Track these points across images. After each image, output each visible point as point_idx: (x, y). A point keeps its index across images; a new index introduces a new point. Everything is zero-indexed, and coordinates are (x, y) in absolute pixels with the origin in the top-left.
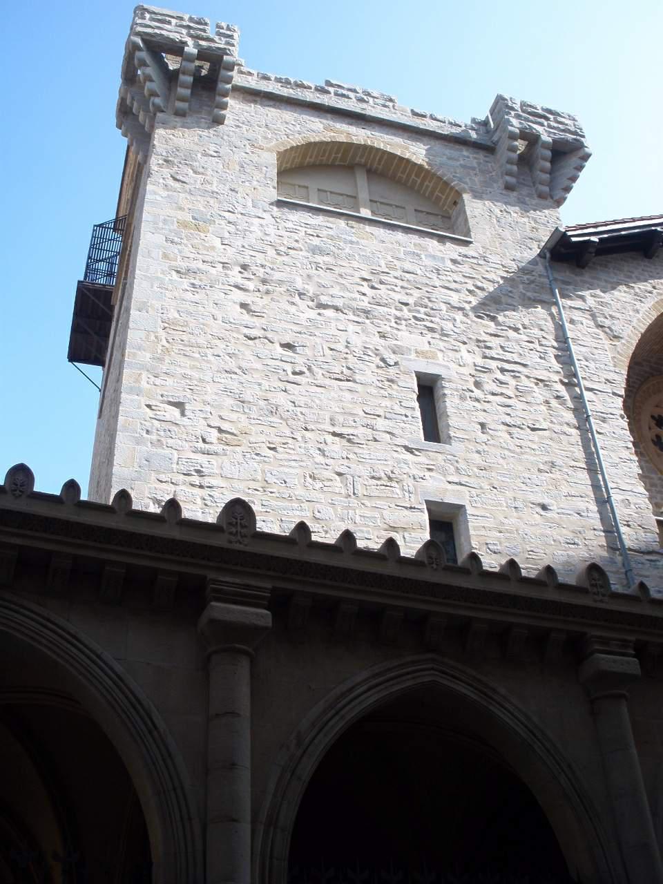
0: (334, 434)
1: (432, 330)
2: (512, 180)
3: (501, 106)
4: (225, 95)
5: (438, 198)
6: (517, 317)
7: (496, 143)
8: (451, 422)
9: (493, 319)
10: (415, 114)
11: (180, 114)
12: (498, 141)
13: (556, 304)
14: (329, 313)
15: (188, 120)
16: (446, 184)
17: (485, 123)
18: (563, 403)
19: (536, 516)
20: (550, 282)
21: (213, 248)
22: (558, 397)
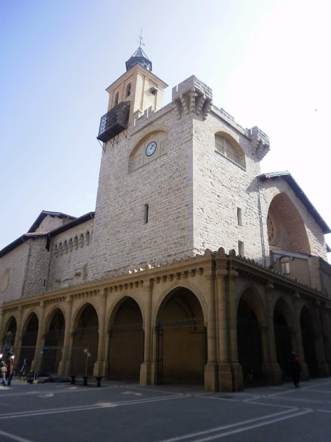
0: (226, 221)
1: (239, 195)
2: (254, 152)
3: (255, 129)
4: (208, 113)
5: (238, 152)
6: (252, 194)
7: (252, 140)
8: (267, 236)
9: (249, 194)
10: (238, 125)
11: (197, 115)
12: (252, 140)
13: (259, 192)
14: (224, 187)
15: (199, 117)
16: (242, 150)
17: (249, 131)
18: (258, 219)
19: (252, 246)
20: (258, 185)
22: (257, 217)
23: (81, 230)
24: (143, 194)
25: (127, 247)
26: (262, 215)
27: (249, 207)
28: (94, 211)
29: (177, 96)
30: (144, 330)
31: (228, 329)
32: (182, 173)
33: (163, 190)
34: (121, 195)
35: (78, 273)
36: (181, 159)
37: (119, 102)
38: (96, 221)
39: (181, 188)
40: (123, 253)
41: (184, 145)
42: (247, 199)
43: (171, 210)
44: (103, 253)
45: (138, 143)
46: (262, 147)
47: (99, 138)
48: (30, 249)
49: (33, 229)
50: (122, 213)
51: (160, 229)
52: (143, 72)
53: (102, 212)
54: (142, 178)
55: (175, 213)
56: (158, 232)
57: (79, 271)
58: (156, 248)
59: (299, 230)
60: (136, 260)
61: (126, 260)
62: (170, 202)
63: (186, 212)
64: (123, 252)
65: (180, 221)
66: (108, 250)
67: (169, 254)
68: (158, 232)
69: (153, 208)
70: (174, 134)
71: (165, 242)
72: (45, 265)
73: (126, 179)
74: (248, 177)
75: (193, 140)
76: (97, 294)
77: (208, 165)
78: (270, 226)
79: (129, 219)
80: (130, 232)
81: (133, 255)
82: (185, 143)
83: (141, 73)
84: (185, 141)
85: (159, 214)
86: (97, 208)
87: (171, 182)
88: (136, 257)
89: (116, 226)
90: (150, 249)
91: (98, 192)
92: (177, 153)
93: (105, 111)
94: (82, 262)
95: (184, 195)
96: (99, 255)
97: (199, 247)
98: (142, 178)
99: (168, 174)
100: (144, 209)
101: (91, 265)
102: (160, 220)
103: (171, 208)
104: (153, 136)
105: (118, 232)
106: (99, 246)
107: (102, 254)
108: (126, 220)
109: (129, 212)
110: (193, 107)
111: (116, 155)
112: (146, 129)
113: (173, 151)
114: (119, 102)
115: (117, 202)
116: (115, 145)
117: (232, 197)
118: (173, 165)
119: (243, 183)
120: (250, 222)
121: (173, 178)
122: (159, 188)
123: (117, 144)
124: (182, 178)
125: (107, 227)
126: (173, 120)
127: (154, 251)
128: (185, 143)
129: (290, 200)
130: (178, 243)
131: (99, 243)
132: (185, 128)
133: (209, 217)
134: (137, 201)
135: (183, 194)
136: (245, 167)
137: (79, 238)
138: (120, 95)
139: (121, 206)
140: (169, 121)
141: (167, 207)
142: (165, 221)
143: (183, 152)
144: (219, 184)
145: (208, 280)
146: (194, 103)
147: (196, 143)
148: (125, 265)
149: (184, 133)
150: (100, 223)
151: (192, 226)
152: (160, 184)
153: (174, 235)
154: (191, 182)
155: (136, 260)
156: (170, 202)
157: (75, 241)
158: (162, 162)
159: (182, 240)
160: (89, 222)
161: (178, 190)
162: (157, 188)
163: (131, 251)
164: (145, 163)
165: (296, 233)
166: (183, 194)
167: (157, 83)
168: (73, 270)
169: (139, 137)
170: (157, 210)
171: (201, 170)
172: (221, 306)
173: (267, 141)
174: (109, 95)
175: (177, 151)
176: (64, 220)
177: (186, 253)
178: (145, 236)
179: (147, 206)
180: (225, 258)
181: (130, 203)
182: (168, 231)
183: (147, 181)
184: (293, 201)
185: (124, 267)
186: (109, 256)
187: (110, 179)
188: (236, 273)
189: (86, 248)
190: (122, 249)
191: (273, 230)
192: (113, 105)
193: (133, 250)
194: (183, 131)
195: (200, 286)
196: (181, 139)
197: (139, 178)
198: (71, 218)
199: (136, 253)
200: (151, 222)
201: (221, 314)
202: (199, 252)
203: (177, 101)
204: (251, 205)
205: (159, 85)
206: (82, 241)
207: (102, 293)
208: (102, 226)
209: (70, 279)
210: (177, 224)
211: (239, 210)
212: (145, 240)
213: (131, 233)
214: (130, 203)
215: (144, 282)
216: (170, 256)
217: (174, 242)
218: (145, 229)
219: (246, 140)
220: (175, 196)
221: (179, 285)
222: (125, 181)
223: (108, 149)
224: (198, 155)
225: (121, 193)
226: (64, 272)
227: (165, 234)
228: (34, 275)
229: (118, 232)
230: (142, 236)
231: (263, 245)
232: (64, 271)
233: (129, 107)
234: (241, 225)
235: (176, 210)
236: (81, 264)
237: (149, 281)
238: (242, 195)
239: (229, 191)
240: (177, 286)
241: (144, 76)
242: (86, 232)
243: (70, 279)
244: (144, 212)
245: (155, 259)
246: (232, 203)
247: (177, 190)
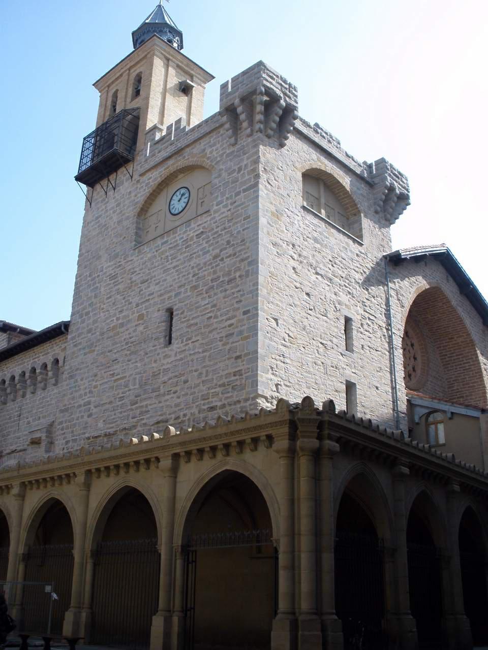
0: (321, 343)
1: (349, 293)
2: (379, 209)
3: (381, 163)
4: (288, 133)
5: (347, 208)
6: (374, 290)
7: (375, 184)
9: (367, 290)
10: (347, 155)
11: (269, 137)
12: (377, 184)
13: (387, 285)
14: (319, 277)
15: (271, 141)
16: (356, 205)
17: (370, 166)
18: (385, 339)
21: (282, 231)
22: (384, 335)
23: (43, 355)
24: (163, 287)
25: (130, 390)
26: (393, 330)
27: (367, 315)
28: (69, 320)
29: (230, 100)
30: (159, 551)
31: (317, 551)
32: (239, 249)
33: (200, 282)
34: (121, 290)
35: (36, 438)
36: (236, 223)
38: (73, 338)
39: (235, 278)
40: (123, 401)
41: (242, 195)
42: (365, 300)
43: (215, 320)
44: (86, 400)
45: (154, 188)
46: (395, 199)
47: (79, 178)
50: (122, 325)
51: (195, 357)
52: (165, 50)
53: (83, 322)
54: (162, 258)
55: (223, 326)
56: (190, 363)
57: (37, 435)
58: (187, 394)
59: (466, 360)
60: (148, 416)
61: (128, 415)
62: (215, 306)
63: (245, 325)
64: (123, 400)
65: (233, 343)
66: (94, 397)
67: (211, 405)
68: (190, 363)
69: (182, 316)
70: (224, 174)
71: (203, 382)
73: (130, 259)
74: (366, 257)
75: (260, 186)
76: (72, 482)
77: (289, 235)
78: (409, 351)
79: (136, 336)
80: (136, 362)
81: (142, 407)
82: (244, 191)
83: (162, 53)
84: (245, 187)
85: (193, 328)
86: (72, 315)
87: (217, 266)
88: (149, 411)
89: (110, 349)
90: (175, 395)
91: (76, 283)
92: (229, 210)
93: (91, 126)
94: (44, 417)
95: (241, 293)
96: (76, 405)
97: (268, 394)
98: (162, 258)
99: (211, 252)
100: (164, 318)
101: (61, 423)
102: (194, 339)
103: (216, 317)
104: (182, 175)
105: (113, 361)
106: (77, 388)
107: (82, 402)
108: (130, 338)
109: (137, 323)
110: (260, 122)
111: (111, 212)
112: (170, 162)
113: (221, 206)
115: (114, 304)
116: (111, 193)
117: (334, 296)
118: (220, 234)
119: (357, 269)
120: (370, 344)
121: (220, 258)
122: (194, 279)
123: (114, 189)
124: (238, 259)
125: (94, 351)
126: (221, 146)
127: (181, 399)
128: (243, 192)
129: (449, 302)
130: (228, 385)
131: (76, 381)
132: (245, 162)
133: (289, 336)
134: (152, 302)
135: (239, 291)
136: (361, 237)
137: (38, 371)
138: (121, 95)
139: (121, 312)
140: (214, 148)
141: (210, 315)
142: (204, 342)
143: (239, 208)
144: (309, 270)
145: (282, 459)
146: (262, 114)
147: (266, 192)
148: (127, 426)
149: (242, 172)
150: (80, 343)
151: (256, 352)
152: (196, 269)
153: (221, 368)
154: (255, 266)
155: (148, 416)
156: (215, 306)
157: (30, 377)
159: (237, 380)
160: (57, 340)
161: (230, 281)
162: (191, 279)
163: (139, 398)
164: (168, 229)
165: (461, 364)
166: (239, 291)
167: (192, 72)
168: (27, 432)
169: (156, 176)
170: (188, 320)
172: (305, 509)
173: (404, 188)
174: (100, 94)
175: (230, 207)
176: (9, 334)
177: (242, 404)
178: (166, 371)
179: (170, 312)
180: (315, 417)
181: (137, 305)
183: (172, 263)
184: (454, 303)
185: (125, 429)
186: (95, 407)
187: (99, 258)
188: (336, 446)
189: (53, 391)
190: (123, 393)
191: (415, 359)
192: (108, 113)
193: (143, 397)
194: (240, 169)
195: (265, 469)
196: (237, 183)
197: (155, 256)
198: (24, 332)
199: (148, 402)
200: (178, 343)
201: (305, 524)
202: (268, 402)
203: (229, 110)
204: (372, 312)
205: (196, 77)
206: (44, 377)
207: (81, 478)
208: (84, 348)
210: (228, 347)
211: (348, 320)
212: (166, 378)
213: (139, 365)
214: (137, 305)
215: (161, 460)
216: (212, 409)
217: (221, 382)
218: (166, 355)
219: (363, 186)
220: (223, 294)
221: (228, 467)
222: (127, 262)
223: (96, 199)
224: (270, 215)
225: (121, 287)
226: (9, 437)
227: (205, 367)
229: (113, 361)
230: (160, 370)
231: (394, 388)
232: (9, 435)
233: (137, 118)
234: (352, 351)
235: (226, 321)
237: (170, 458)
238: (355, 293)
239: (329, 284)
240: (224, 469)
241: (168, 60)
242: (52, 360)
243: (21, 451)
244: (163, 324)
245: (185, 415)
246: (335, 307)
247: (228, 282)
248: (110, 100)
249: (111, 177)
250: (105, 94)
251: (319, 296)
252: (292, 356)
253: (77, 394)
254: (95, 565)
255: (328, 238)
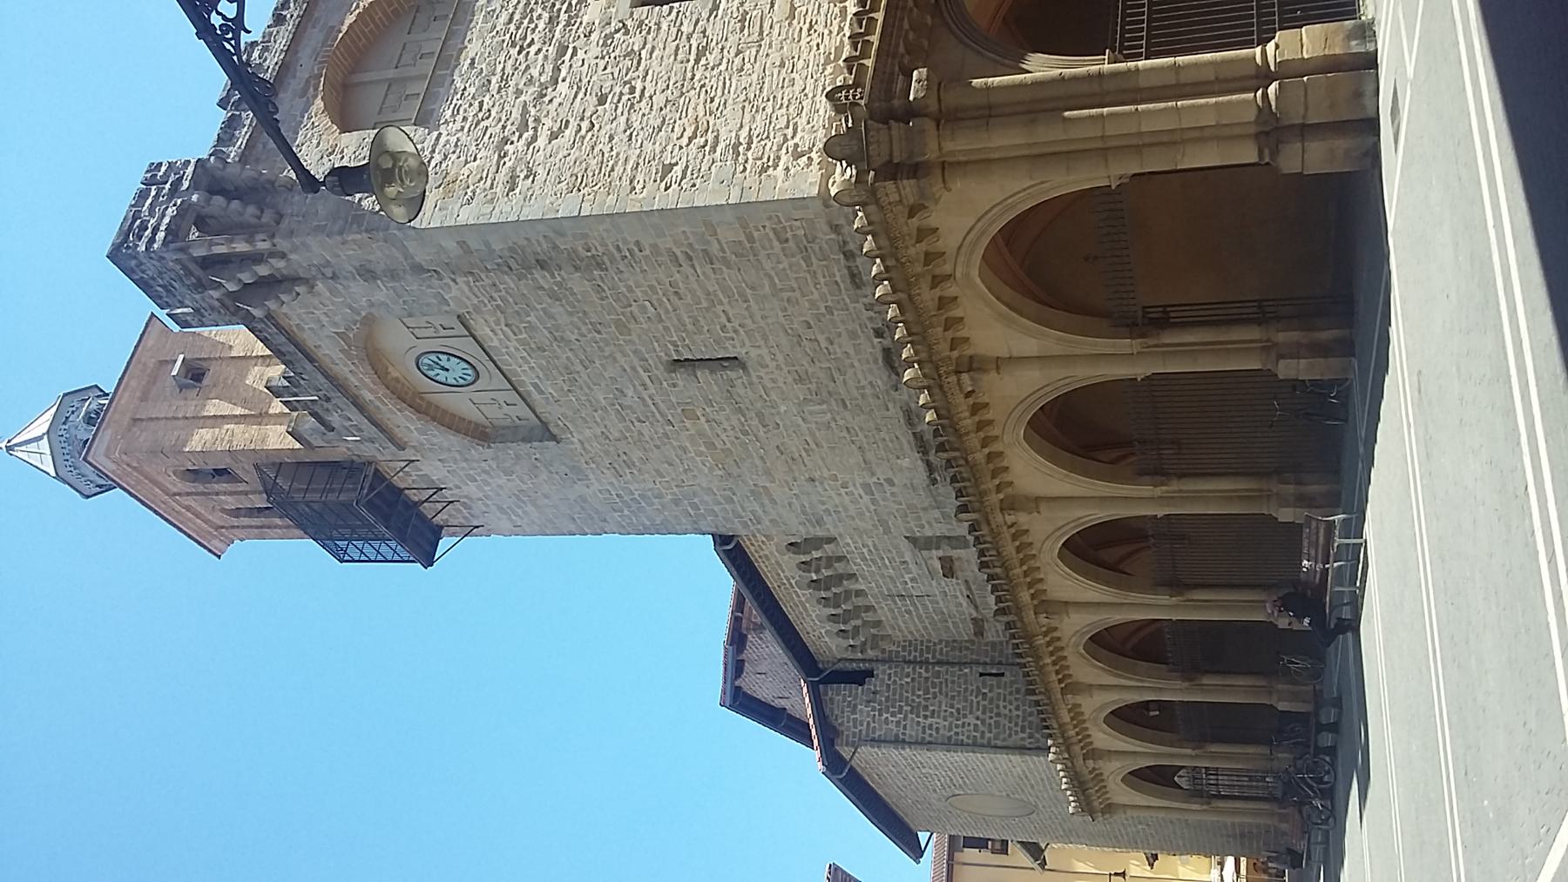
0: (697, 61)
37: (260, 502)
38: (745, 525)
48: (877, 742)
49: (794, 728)
66: (853, 481)
72: (927, 679)
73: (579, 446)
93: (307, 551)
97: (815, 174)
102: (724, 319)
107: (866, 498)
114: (260, 502)
117: (594, 36)
131: (826, 511)
140: (325, 319)
142: (725, 301)
157: (827, 589)
158: (497, 328)
160: (750, 550)
171: (512, 184)
176: (748, 629)
182: (763, 287)
186: (873, 474)
189: (847, 545)
192: (278, 521)
209: (969, 589)
221: (975, 273)
228: (965, 716)
233: (280, 467)
236: (907, 559)
239: (570, 51)
240: (978, 281)
243: (969, 589)
244: (699, 373)
246: (617, 31)
248: (245, 521)
249: (415, 496)
250: (236, 531)
251: (600, 72)
252: (734, 124)
253: (852, 507)
254: (1197, 586)
255: (473, 60)
